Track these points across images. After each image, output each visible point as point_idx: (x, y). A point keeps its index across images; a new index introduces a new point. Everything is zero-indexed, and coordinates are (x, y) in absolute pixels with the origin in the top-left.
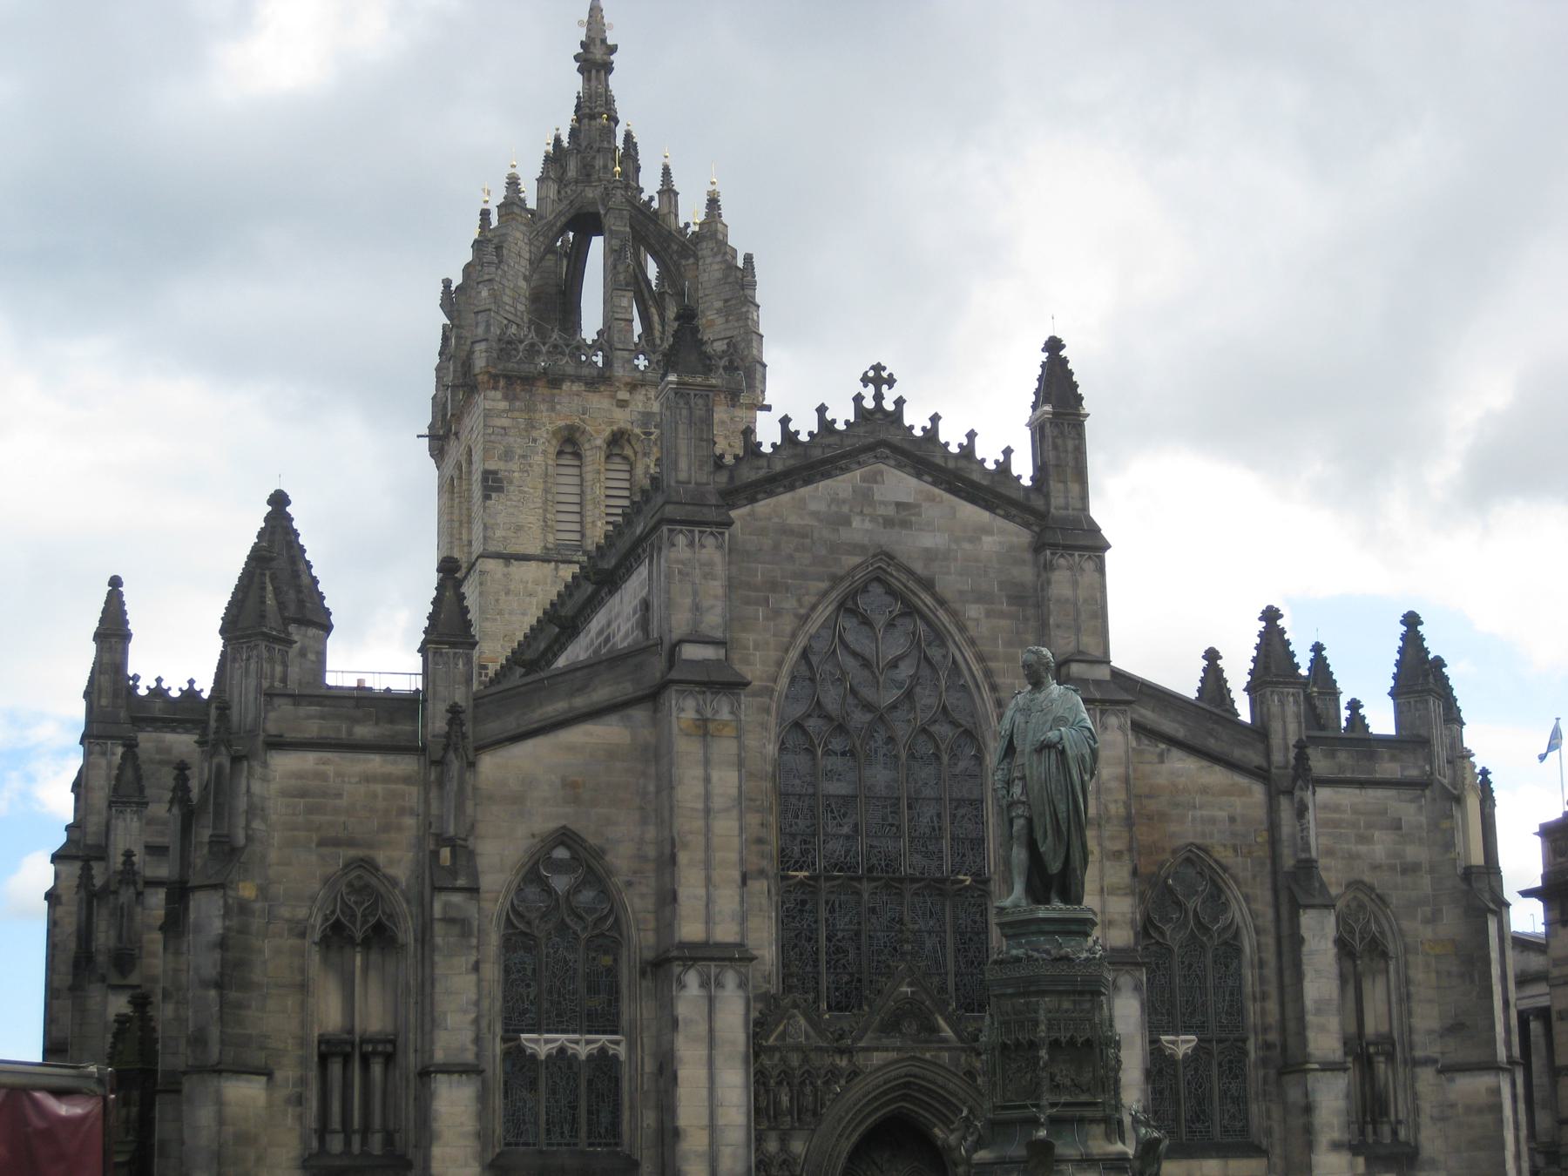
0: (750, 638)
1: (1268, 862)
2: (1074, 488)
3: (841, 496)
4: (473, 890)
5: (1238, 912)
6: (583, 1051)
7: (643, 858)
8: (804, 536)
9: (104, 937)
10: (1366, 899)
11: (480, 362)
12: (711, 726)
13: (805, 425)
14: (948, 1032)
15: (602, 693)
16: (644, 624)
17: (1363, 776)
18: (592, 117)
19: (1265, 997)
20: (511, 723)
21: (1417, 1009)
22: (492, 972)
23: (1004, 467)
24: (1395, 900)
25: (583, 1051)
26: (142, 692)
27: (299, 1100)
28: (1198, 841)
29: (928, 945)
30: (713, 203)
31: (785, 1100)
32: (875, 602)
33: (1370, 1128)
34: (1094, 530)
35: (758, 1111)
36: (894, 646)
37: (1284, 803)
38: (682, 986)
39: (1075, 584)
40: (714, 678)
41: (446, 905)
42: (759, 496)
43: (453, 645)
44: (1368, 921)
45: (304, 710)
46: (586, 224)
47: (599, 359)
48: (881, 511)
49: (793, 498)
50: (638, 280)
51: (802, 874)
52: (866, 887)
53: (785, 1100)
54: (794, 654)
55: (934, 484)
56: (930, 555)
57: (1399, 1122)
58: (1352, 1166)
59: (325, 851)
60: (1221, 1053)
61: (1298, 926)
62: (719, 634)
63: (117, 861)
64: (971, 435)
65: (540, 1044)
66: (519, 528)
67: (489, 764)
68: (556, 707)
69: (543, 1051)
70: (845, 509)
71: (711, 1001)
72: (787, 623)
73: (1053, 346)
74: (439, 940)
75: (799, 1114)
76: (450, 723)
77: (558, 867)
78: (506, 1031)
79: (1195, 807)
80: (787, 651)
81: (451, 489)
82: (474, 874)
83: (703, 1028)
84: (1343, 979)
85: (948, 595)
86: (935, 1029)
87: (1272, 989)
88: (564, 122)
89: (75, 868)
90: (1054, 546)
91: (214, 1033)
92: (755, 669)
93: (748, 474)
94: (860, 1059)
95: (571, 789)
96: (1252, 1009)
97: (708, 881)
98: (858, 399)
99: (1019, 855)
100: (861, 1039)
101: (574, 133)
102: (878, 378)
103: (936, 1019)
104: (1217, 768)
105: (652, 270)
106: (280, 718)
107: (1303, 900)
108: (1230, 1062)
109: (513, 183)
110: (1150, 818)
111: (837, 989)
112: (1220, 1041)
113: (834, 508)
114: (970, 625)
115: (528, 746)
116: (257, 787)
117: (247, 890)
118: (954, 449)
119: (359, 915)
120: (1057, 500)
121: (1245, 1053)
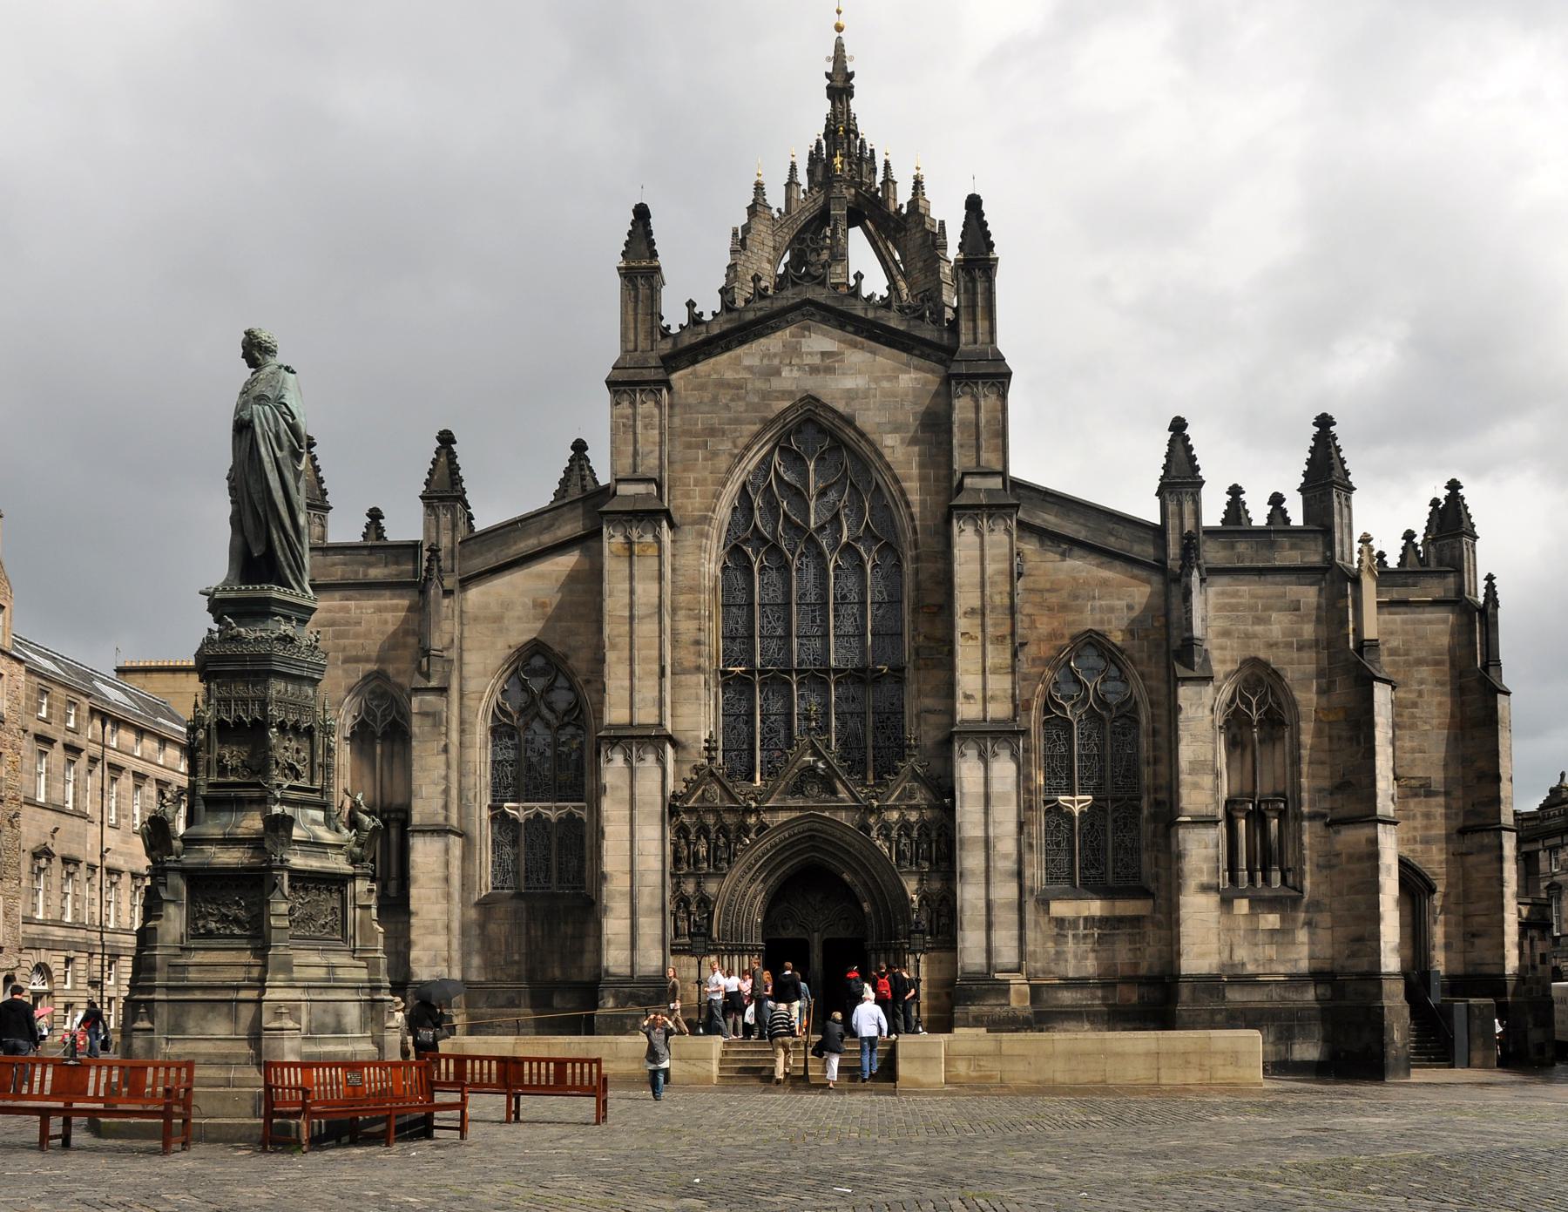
0: (692, 476)
1: (1164, 643)
3: (772, 350)
8: (740, 387)
10: (1264, 676)
12: (636, 548)
14: (843, 794)
17: (1261, 565)
19: (1156, 761)
24: (1290, 674)
28: (1096, 628)
29: (850, 724)
31: (703, 851)
33: (1259, 874)
35: (677, 860)
39: (977, 409)
40: (639, 507)
41: (421, 701)
42: (700, 358)
43: (441, 499)
44: (1266, 693)
48: (808, 360)
49: (730, 357)
51: (737, 669)
53: (703, 851)
54: (732, 489)
55: (855, 333)
56: (851, 395)
57: (1289, 870)
59: (346, 666)
60: (1114, 811)
67: (474, 594)
69: (521, 816)
70: (776, 362)
71: (632, 770)
72: (723, 463)
74: (415, 729)
75: (715, 861)
76: (429, 560)
77: (534, 673)
78: (494, 801)
79: (1094, 598)
80: (724, 486)
86: (834, 792)
87: (1164, 755)
90: (959, 376)
92: (686, 500)
93: (688, 340)
94: (766, 818)
96: (1146, 772)
97: (632, 673)
100: (767, 801)
103: (834, 784)
104: (1117, 563)
108: (1124, 818)
110: (1050, 609)
111: (769, 762)
112: (1114, 800)
113: (766, 362)
114: (887, 453)
119: (379, 714)
121: (1138, 810)
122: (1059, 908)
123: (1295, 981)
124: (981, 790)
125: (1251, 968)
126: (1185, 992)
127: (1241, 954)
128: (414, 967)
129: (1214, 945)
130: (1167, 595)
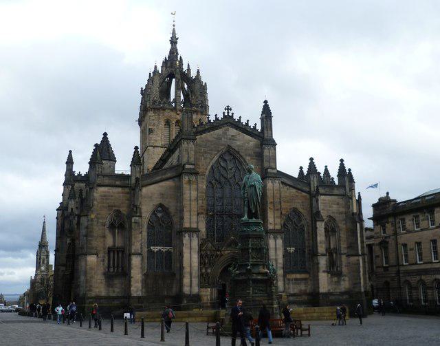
2: (269, 132)
4: (140, 216)
5: (303, 222)
6: (164, 250)
7: (177, 210)
9: (67, 226)
11: (148, 106)
13: (212, 118)
15: (169, 175)
16: (178, 161)
18: (173, 53)
20: (149, 181)
21: (342, 243)
22: (145, 234)
23: (255, 128)
24: (337, 219)
25: (164, 250)
26: (76, 175)
27: (103, 261)
30: (198, 71)
32: (227, 157)
34: (274, 141)
36: (230, 165)
37: (314, 199)
38: (185, 237)
45: (105, 178)
46: (172, 76)
47: (174, 105)
50: (183, 88)
52: (224, 217)
54: (209, 167)
56: (239, 146)
58: (328, 276)
61: (316, 225)
62: (193, 163)
63: (70, 210)
64: (248, 121)
65: (155, 249)
66: (156, 141)
67: (144, 190)
68: (158, 178)
73: (266, 102)
77: (159, 212)
81: (143, 132)
82: (141, 213)
83: (189, 246)
84: (326, 236)
85: (242, 154)
88: (167, 54)
89: (60, 212)
91: (85, 246)
93: (200, 129)
95: (162, 195)
96: (307, 244)
98: (224, 113)
99: (246, 209)
101: (169, 57)
102: (228, 109)
105: (186, 86)
106: (99, 181)
107: (317, 219)
109: (156, 67)
115: (153, 185)
116: (95, 194)
117: (93, 216)
118: (244, 124)
120: (266, 135)
122: (289, 276)
123: (342, 294)
124: (274, 246)
125: (331, 291)
126: (321, 298)
127: (330, 288)
128: (132, 292)
129: (326, 286)
130: (311, 200)
